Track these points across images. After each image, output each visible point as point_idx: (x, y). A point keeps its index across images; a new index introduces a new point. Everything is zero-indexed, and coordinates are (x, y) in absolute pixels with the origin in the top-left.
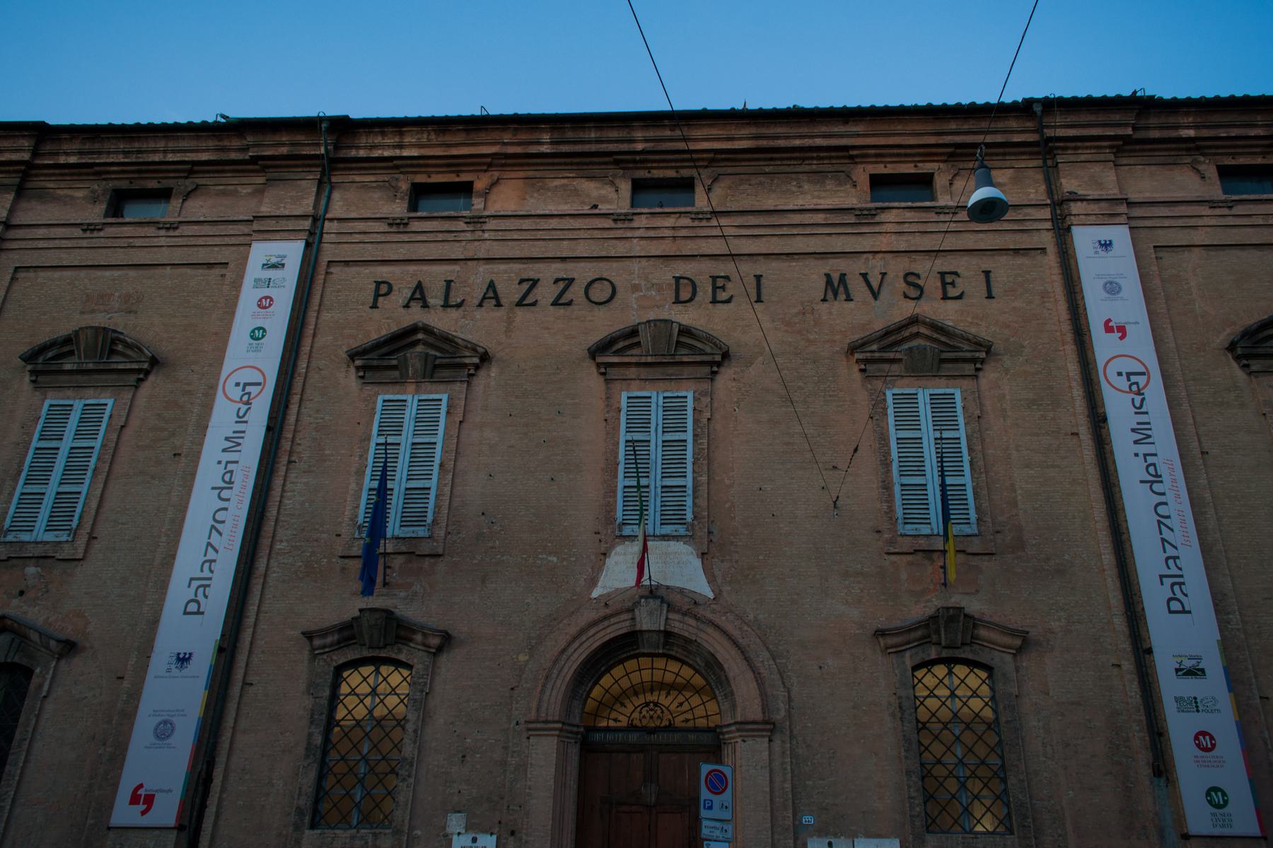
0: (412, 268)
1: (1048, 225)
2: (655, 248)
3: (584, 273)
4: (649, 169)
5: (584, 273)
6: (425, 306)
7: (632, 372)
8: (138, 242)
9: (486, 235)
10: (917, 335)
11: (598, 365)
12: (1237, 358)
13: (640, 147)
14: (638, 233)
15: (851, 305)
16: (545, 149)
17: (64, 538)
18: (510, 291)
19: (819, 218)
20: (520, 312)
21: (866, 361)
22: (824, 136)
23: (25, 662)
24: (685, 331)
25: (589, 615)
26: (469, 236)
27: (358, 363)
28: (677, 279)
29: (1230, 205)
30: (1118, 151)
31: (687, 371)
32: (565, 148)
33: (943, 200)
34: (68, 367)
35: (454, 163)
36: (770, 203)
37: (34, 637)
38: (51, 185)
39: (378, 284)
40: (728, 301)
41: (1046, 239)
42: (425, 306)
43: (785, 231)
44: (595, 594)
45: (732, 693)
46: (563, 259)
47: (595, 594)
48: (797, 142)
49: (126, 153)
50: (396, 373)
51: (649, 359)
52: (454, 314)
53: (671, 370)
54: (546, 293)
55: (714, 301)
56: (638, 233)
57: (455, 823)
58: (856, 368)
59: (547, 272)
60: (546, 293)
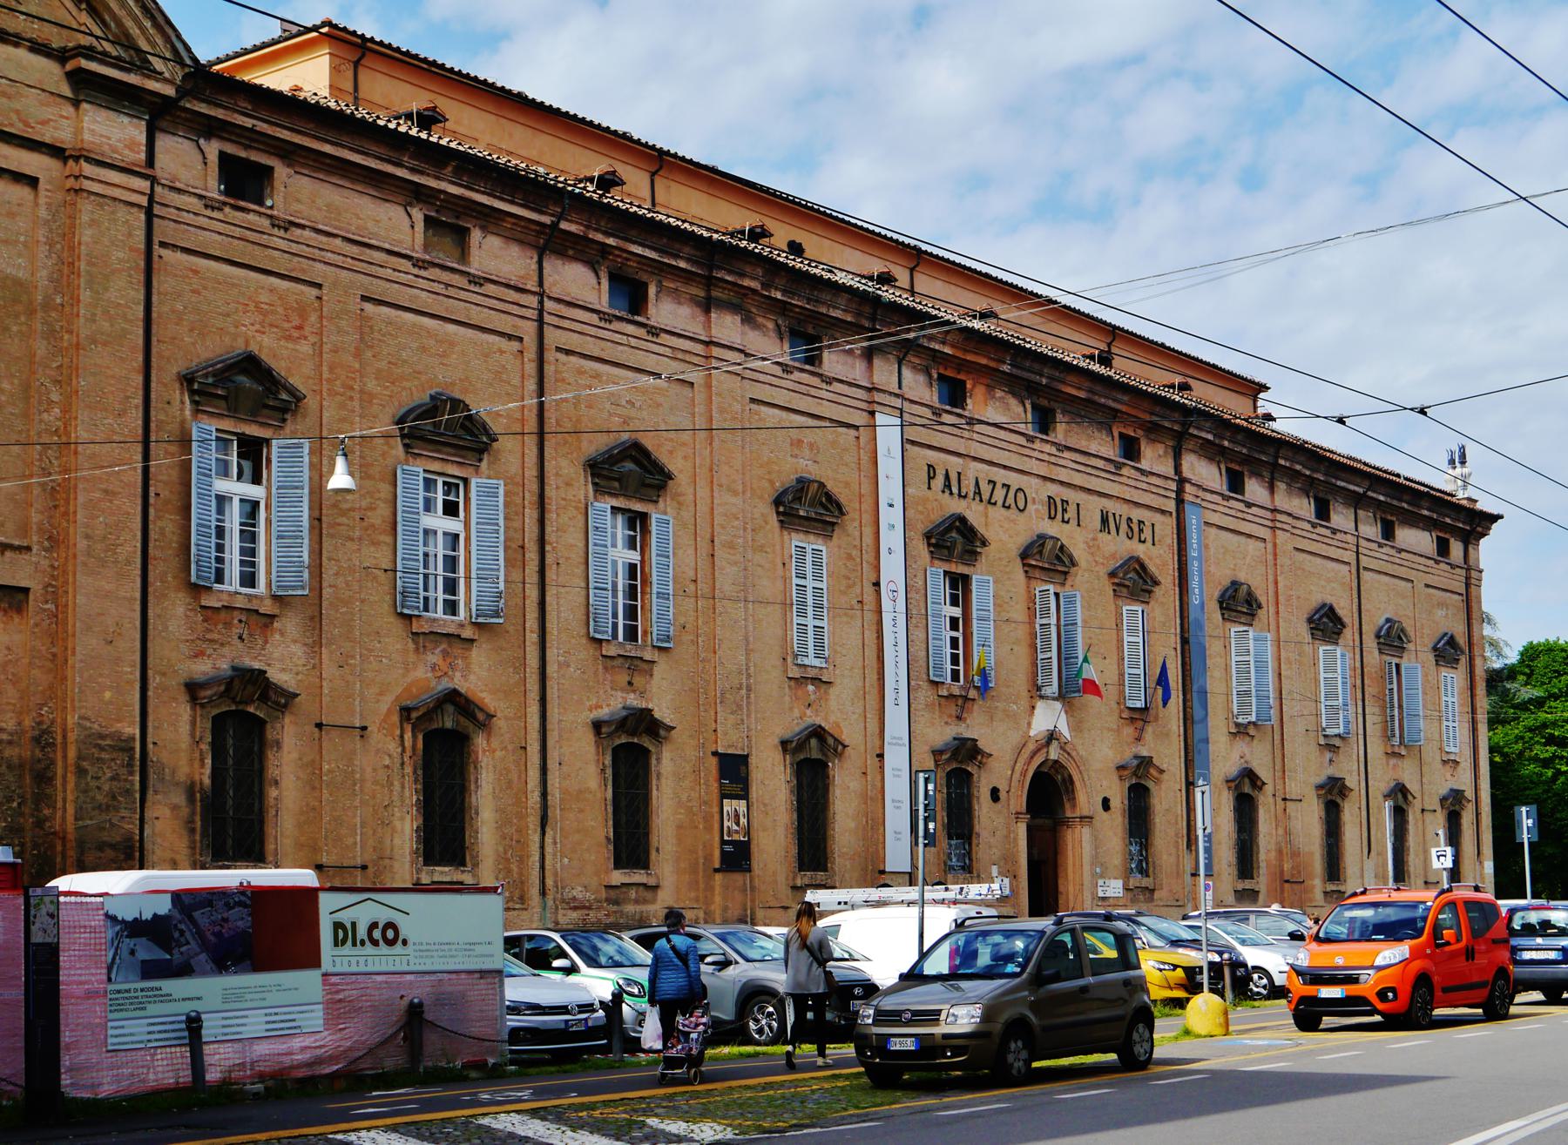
0: (942, 456)
1: (1174, 495)
2: (1043, 470)
3: (1015, 480)
4: (1039, 397)
5: (1015, 480)
6: (951, 493)
7: (1037, 574)
8: (813, 392)
9: (975, 436)
10: (1135, 569)
11: (1024, 565)
12: (1221, 608)
13: (1044, 381)
14: (1036, 454)
15: (1109, 537)
16: (1006, 368)
17: (824, 665)
18: (985, 489)
19: (1100, 464)
20: (990, 506)
21: (1118, 585)
22: (1115, 400)
23: (824, 758)
24: (1062, 546)
25: (1031, 747)
26: (966, 434)
27: (933, 541)
28: (1049, 497)
29: (1228, 498)
30: (1202, 447)
31: (1057, 576)
32: (1015, 371)
33: (1144, 464)
34: (802, 513)
35: (962, 365)
36: (1082, 444)
37: (831, 741)
38: (754, 310)
39: (929, 466)
40: (1068, 522)
41: (1171, 506)
42: (951, 493)
43: (1089, 470)
44: (1032, 733)
45: (1074, 798)
46: (1005, 467)
47: (1032, 733)
48: (1103, 400)
49: (809, 301)
50: (946, 552)
51: (1046, 566)
52: (963, 503)
53: (1051, 574)
54: (999, 495)
55: (1063, 521)
56: (1036, 454)
57: (995, 870)
58: (1112, 588)
59: (1001, 476)
60: (999, 495)
